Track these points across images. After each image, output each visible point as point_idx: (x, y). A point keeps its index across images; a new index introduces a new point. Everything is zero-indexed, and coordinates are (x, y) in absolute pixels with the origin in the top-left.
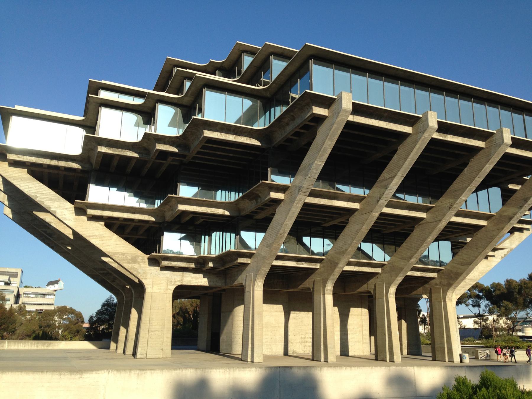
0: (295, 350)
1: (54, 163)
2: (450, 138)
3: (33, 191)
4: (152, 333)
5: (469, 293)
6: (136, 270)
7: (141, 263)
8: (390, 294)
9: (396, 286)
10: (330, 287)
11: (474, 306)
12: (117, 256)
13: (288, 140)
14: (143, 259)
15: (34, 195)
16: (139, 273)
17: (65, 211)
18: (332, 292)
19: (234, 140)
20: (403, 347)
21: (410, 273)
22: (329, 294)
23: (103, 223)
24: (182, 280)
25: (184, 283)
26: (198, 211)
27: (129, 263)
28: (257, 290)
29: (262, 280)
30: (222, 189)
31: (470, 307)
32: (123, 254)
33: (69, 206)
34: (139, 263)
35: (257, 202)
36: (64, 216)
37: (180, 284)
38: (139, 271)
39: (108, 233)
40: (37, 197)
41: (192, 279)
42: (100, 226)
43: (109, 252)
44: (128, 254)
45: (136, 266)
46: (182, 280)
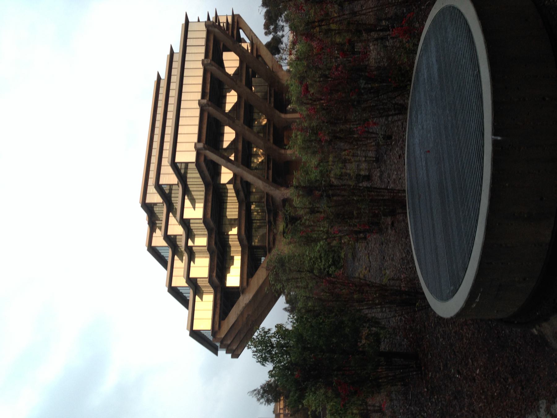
1: (218, 306)
2: (208, 90)
5: (272, 33)
10: (283, 151)
11: (283, 31)
13: (210, 174)
15: (236, 315)
17: (245, 299)
21: (272, 105)
22: (286, 151)
23: (250, 279)
31: (284, 33)
33: (241, 298)
39: (256, 277)
40: (238, 314)
42: (252, 281)
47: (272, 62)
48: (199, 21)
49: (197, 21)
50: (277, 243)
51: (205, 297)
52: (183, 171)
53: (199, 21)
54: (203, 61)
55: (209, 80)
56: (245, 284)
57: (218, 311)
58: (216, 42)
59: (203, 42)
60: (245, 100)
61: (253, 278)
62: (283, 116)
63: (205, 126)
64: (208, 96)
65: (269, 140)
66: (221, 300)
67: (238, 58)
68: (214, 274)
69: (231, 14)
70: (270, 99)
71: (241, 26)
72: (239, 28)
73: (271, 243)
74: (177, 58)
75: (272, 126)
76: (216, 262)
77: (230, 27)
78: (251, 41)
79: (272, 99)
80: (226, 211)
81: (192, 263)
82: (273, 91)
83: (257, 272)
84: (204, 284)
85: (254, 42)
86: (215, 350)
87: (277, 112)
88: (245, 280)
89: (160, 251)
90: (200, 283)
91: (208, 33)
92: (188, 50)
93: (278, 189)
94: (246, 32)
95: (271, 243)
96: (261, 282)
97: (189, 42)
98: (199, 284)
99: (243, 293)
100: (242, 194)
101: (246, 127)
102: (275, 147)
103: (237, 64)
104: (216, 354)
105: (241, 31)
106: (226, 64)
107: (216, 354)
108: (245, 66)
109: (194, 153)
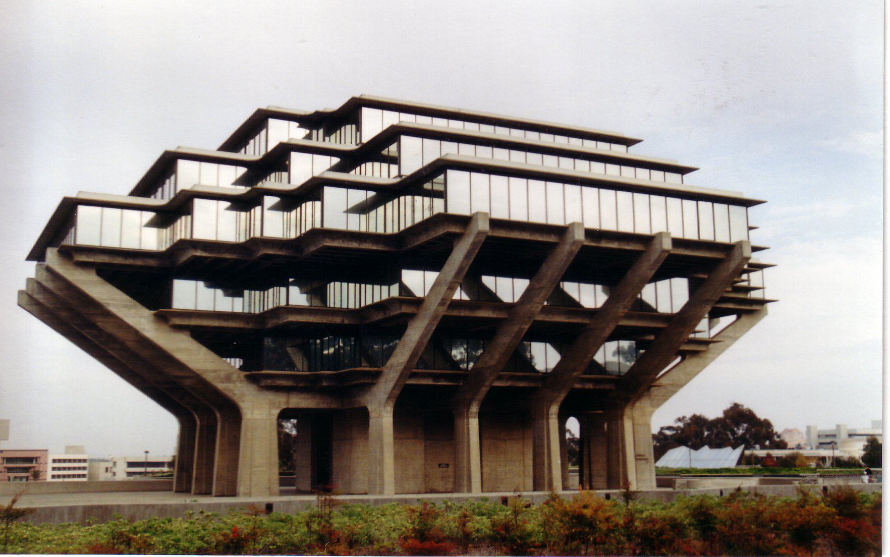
0: (433, 487)
1: (129, 262)
2: (604, 244)
3: (105, 297)
4: (256, 469)
6: (230, 391)
7: (237, 383)
8: (552, 414)
9: (559, 404)
10: (474, 409)
12: (208, 374)
14: (239, 377)
15: (105, 301)
16: (235, 394)
17: (143, 321)
18: (477, 415)
19: (358, 247)
20: (584, 479)
21: (577, 386)
22: (475, 417)
24: (287, 403)
25: (291, 406)
26: (311, 321)
27: (222, 382)
28: (386, 416)
29: (391, 405)
30: (335, 281)
32: (215, 371)
33: (147, 313)
34: (234, 382)
35: (385, 314)
36: (143, 327)
37: (284, 407)
38: (236, 392)
41: (300, 401)
43: (198, 370)
44: (220, 370)
45: (231, 386)
46: (287, 403)
47: (671, 385)
48: (750, 228)
49: (751, 225)
50: (270, 396)
51: (153, 231)
52: (428, 186)
53: (750, 228)
54: (668, 234)
55: (627, 247)
56: (177, 321)
57: (118, 260)
58: (709, 265)
59: (707, 236)
60: (586, 324)
61: (191, 339)
62: (554, 409)
63: (526, 236)
64: (593, 244)
65: (500, 378)
66: (141, 267)
67: (676, 310)
68: (199, 253)
69: (767, 298)
70: (589, 381)
71: (744, 319)
72: (739, 314)
73: (269, 382)
74: (672, 181)
75: (532, 385)
76: (227, 256)
77: (742, 296)
78: (715, 339)
79: (589, 386)
80: (341, 281)
81: (228, 204)
82: (608, 387)
83: (204, 350)
84: (181, 229)
85: (711, 346)
86: (37, 254)
87: (562, 396)
88: (185, 322)
89: (257, 138)
90: (182, 223)
91: (728, 249)
92: (690, 204)
93: (389, 398)
94: (731, 328)
95: (269, 382)
96: (181, 357)
97: (705, 206)
98: (179, 221)
99: (155, 315)
100: (378, 316)
101: (527, 327)
102: (484, 390)
103: (664, 308)
104: (30, 257)
105: (732, 318)
106: (663, 285)
107: (30, 257)
108: (661, 325)
109: (465, 212)
